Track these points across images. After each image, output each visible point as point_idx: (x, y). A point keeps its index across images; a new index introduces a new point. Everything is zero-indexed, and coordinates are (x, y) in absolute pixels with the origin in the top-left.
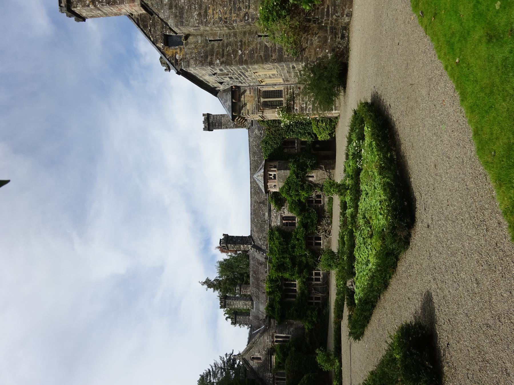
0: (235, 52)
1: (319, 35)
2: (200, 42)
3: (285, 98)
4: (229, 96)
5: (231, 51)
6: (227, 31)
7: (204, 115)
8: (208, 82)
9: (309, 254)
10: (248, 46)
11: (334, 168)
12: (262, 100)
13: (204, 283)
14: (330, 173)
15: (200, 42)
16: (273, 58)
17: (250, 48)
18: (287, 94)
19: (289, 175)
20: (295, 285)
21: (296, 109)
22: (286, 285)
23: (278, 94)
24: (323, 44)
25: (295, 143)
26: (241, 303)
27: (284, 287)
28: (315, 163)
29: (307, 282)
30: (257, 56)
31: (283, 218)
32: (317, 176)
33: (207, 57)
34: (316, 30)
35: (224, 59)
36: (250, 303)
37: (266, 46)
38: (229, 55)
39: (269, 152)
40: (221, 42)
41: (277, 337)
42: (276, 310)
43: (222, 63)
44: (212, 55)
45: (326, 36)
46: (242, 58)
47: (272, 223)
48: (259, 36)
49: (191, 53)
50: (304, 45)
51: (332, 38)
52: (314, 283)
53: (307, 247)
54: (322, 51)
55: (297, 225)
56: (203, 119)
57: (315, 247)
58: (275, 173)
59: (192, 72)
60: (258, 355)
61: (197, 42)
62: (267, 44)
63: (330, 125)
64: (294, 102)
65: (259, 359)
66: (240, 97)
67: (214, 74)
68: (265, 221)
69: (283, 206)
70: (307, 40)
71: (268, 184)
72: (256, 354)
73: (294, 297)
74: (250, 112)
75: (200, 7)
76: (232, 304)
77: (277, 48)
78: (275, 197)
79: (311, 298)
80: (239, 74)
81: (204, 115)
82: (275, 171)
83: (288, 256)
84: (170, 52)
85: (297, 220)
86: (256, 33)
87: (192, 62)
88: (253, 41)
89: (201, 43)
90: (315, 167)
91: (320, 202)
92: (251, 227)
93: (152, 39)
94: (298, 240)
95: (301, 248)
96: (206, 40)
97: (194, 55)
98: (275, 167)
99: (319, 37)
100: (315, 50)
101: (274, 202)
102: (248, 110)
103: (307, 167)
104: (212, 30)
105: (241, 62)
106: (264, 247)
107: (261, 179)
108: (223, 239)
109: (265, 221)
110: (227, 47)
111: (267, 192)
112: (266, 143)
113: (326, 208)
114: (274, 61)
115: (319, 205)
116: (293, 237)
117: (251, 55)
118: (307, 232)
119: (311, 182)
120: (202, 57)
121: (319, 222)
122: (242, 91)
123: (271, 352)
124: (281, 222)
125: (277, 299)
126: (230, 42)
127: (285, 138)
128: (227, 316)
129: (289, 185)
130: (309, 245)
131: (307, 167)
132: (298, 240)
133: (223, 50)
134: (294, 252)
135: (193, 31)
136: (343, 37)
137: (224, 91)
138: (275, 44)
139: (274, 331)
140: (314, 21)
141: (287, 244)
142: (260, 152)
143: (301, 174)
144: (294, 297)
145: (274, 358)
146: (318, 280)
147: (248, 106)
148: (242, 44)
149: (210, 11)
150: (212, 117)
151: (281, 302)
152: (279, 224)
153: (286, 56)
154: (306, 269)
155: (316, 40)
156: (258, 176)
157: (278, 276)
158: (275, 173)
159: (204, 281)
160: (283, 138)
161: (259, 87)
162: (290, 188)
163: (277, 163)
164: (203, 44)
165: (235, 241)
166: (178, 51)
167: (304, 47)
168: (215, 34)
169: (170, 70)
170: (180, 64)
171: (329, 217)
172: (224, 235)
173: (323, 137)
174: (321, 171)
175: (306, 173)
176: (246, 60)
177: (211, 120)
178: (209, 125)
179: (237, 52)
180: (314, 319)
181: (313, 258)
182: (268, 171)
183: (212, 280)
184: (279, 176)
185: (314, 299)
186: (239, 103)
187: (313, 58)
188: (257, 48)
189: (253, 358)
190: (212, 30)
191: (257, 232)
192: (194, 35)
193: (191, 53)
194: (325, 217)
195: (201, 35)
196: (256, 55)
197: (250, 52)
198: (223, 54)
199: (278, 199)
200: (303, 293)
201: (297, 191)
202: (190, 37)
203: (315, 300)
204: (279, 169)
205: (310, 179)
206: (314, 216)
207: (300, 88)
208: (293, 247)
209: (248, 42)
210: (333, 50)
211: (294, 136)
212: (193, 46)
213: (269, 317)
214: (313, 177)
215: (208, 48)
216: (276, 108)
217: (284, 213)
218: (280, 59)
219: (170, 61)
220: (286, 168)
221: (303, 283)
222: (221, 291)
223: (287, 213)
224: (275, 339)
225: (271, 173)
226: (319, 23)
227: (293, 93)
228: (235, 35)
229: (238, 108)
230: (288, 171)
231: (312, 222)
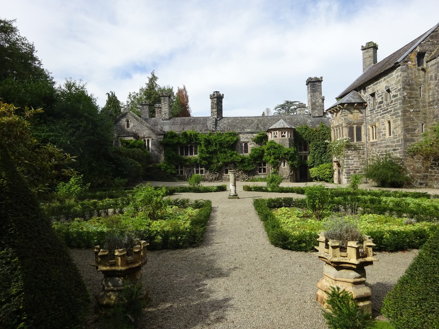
0: (412, 107)
1: (422, 167)
2: (420, 80)
3: (356, 143)
4: (359, 101)
5: (412, 104)
6: (427, 101)
7: (322, 78)
8: (376, 84)
9: (220, 165)
10: (416, 117)
11: (291, 181)
12: (355, 126)
13: (153, 75)
14: (288, 178)
15: (420, 80)
16: (407, 135)
17: (414, 118)
18: (359, 145)
19: (285, 147)
20: (191, 154)
21: (348, 152)
22: (191, 147)
23: (359, 138)
24: (416, 171)
25: (305, 151)
26: (166, 110)
27: (189, 146)
28: (295, 167)
29: (196, 164)
30: (409, 124)
31: (246, 144)
32: (285, 169)
33: (409, 85)
34: (426, 165)
35: (407, 99)
36: (167, 117)
37: (415, 130)
38: (410, 102)
40: (419, 96)
41: (148, 141)
42: (172, 140)
43: (404, 97)
44: (410, 90)
45: (421, 172)
46: (408, 112)
47: (242, 135)
48: (423, 124)
49: (412, 73)
50: (415, 157)
51: (420, 176)
52: (195, 169)
53: (224, 162)
54: (411, 170)
55: (241, 154)
56: (319, 77)
57: (224, 169)
58: (286, 137)
59: (394, 73)
60: (131, 125)
61: (420, 78)
62: (417, 130)
63: (327, 178)
64: (353, 150)
65: (128, 126)
67: (389, 91)
68: (243, 129)
69: (256, 143)
70: (419, 159)
71: (277, 132)
72: (132, 124)
73: (182, 154)
74: (346, 117)
76: (165, 102)
77: (414, 138)
78: (264, 137)
79: (181, 168)
80: (387, 109)
81: (322, 78)
82: (288, 136)
83: (218, 148)
84: (414, 57)
85: (247, 155)
86: (425, 122)
87: (405, 74)
88: (419, 120)
89: (419, 81)
90: (292, 167)
91: (260, 172)
92: (230, 118)
93: (423, 42)
94: (231, 156)
95: (225, 159)
96: (421, 85)
97: (410, 75)
98: (290, 136)
99: (421, 167)
100: (412, 165)
101: (260, 136)
102: (347, 115)
103: (293, 161)
104: (430, 89)
105: (405, 112)
106: (218, 128)
107: (281, 126)
108: (220, 94)
109: (243, 129)
110: (416, 101)
111: (270, 131)
112: (306, 129)
113: (256, 177)
114: (405, 136)
115: (258, 171)
116: (233, 152)
117: (410, 119)
118: (238, 162)
119: (280, 165)
120: (409, 82)
121: (246, 172)
122: (362, 111)
123: (136, 136)
124: (243, 142)
125: (181, 141)
126: (419, 103)
127: (310, 144)
128: (111, 94)
129: (275, 147)
130: (226, 164)
131: (293, 161)
132: (231, 156)
133: (413, 98)
134: (220, 152)
135: (430, 75)
136: (421, 184)
137: (360, 97)
138: (417, 136)
139: (153, 138)
140: (436, 164)
141: (227, 147)
143: (288, 157)
144: (182, 154)
145: (132, 138)
146: (197, 172)
147: (350, 116)
148: (418, 112)
150: (319, 84)
151: (178, 143)
152: (242, 140)
153: (408, 144)
154: (207, 164)
155: (418, 165)
156: (283, 123)
157: (201, 141)
158: (286, 137)
159: (155, 75)
160: (310, 142)
161: (365, 124)
162: (275, 148)
163: (292, 138)
164: (418, 82)
165: (219, 105)
166: (414, 63)
167: (414, 157)
168: (425, 91)
169: (362, 50)
170: (404, 65)
171: (249, 179)
172: (223, 95)
173: (313, 171)
174: (289, 172)
175: (288, 161)
176: (406, 115)
177: (317, 83)
178: (314, 82)
179: (412, 109)
180: (169, 170)
181: (217, 168)
182: (288, 131)
183: (157, 82)
184: (284, 139)
185: (181, 170)
186: (352, 108)
187: (406, 163)
188: (414, 123)
189: (128, 121)
190: (430, 89)
191: (228, 123)
192: (425, 75)
193: (412, 73)
194: (249, 176)
195: (424, 81)
196: (409, 122)
197: (412, 118)
198: (411, 98)
199: (262, 140)
200: (186, 160)
201: (273, 154)
202: (423, 73)
203: (196, 170)
204: (290, 140)
205: (283, 164)
206: (249, 168)
207: (363, 154)
208: (225, 152)
209: (419, 117)
210: (412, 177)
211: (311, 151)
212: (417, 74)
213: (165, 135)
214: (284, 166)
215: (415, 86)
216: (349, 136)
217: (251, 144)
218: (406, 140)
219: (406, 57)
220: (290, 145)
221: (196, 160)
222: (147, 90)
223: (251, 146)
224: (146, 139)
225: (286, 133)
226: (431, 167)
227: (359, 150)
228: (424, 107)
229: (349, 107)
230: (288, 147)
231: (245, 166)
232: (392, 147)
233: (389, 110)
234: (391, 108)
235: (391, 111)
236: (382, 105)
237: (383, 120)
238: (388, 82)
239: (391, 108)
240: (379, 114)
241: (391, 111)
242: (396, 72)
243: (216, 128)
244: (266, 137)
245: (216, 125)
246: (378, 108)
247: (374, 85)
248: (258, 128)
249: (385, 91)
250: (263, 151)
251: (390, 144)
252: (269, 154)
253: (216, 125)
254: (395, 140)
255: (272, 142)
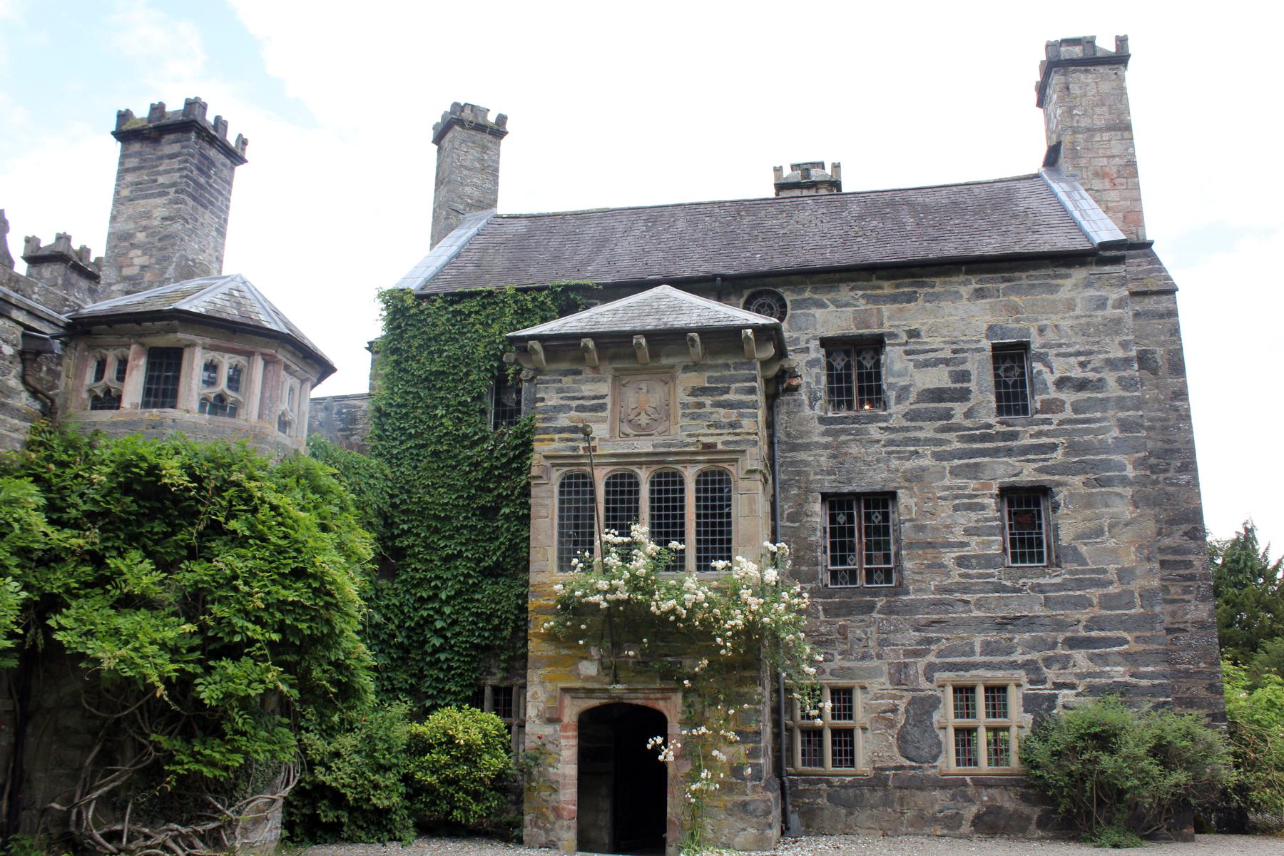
8: (911, 298)
80: (1014, 436)
232: (1060, 625)
233: (1028, 441)
234: (1040, 434)
235: (1054, 447)
236: (959, 409)
237: (973, 484)
238: (1016, 310)
239: (1040, 434)
240: (928, 450)
241: (1054, 447)
242: (1089, 284)
246: (912, 416)
247: (876, 300)
249: (986, 344)
251: (1039, 611)
254: (1094, 594)
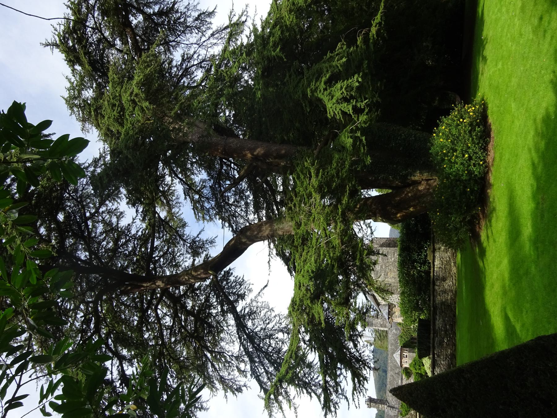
4: (387, 307)
39: (403, 342)
66: (392, 309)
75: (385, 272)
106: (396, 406)
111: (401, 366)
137: (384, 305)
142: (397, 343)
147: (396, 314)
149: (389, 274)
163: (408, 349)
204: (409, 352)
220: (413, 352)
243: (396, 408)
244: (406, 368)
245: (393, 407)
248: (398, 374)
250: (417, 373)
252: (420, 369)
253: (393, 407)
255: (410, 365)
